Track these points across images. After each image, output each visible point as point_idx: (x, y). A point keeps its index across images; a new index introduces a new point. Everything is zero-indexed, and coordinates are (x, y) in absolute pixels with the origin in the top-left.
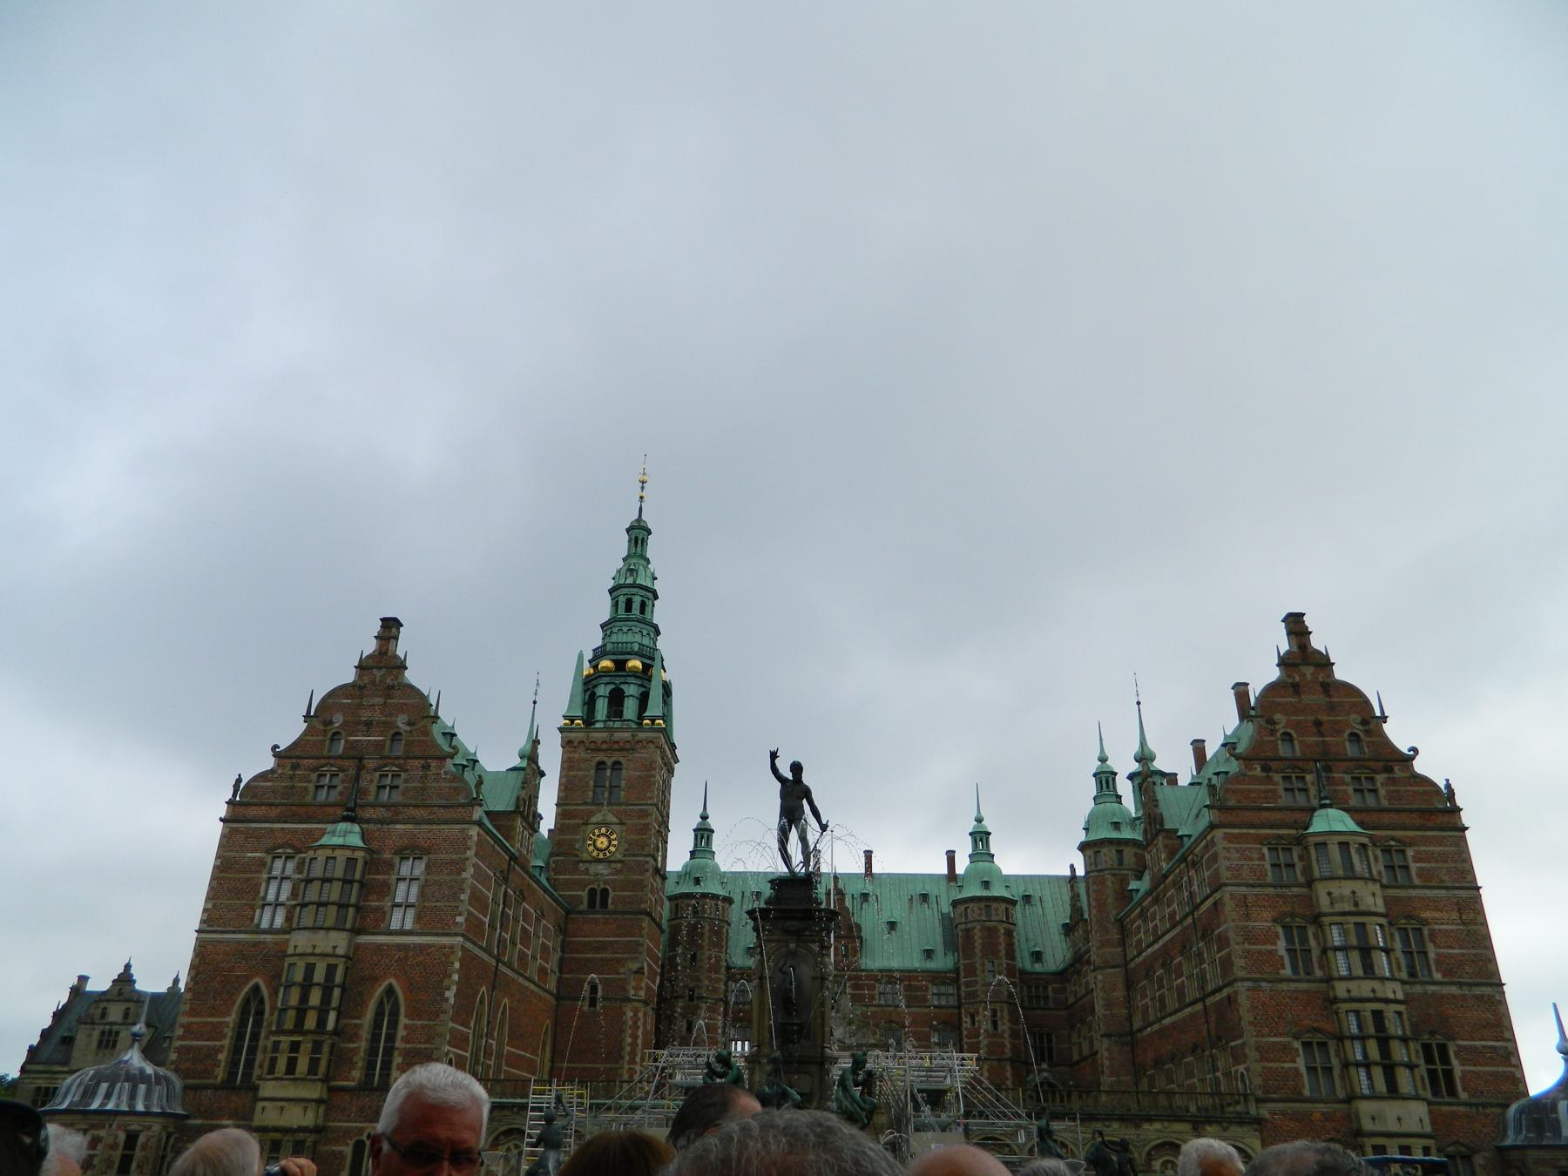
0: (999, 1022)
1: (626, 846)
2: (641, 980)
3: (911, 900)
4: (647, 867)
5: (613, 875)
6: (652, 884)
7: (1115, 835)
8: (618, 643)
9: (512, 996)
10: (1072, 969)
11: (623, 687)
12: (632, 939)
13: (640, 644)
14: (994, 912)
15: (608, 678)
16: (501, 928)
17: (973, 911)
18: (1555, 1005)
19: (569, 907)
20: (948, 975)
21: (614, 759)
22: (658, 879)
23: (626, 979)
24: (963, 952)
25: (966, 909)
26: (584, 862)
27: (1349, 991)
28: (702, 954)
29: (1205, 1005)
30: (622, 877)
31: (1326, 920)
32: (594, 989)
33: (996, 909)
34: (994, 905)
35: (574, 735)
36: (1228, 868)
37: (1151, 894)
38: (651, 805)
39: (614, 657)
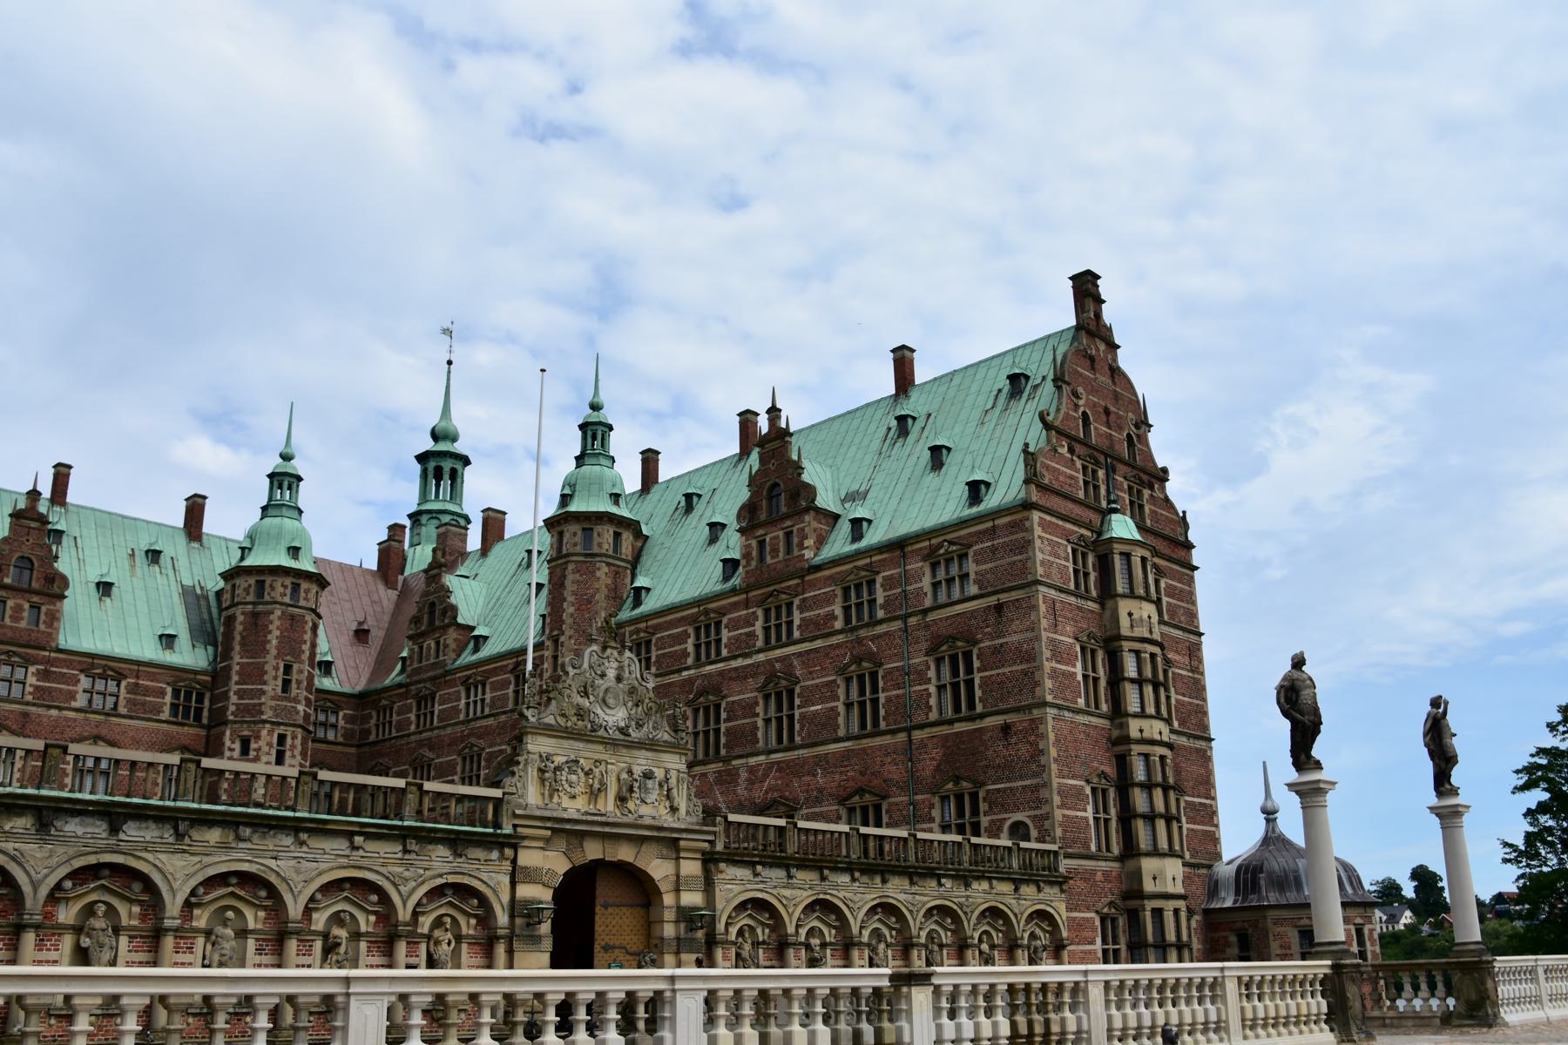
0: (288, 754)
3: (133, 555)
7: (614, 510)
10: (403, 690)
14: (303, 595)
17: (271, 586)
18: (1264, 763)
20: (199, 677)
24: (243, 644)
25: (260, 584)
27: (1141, 731)
29: (910, 740)
31: (1126, 645)
33: (307, 591)
34: (304, 585)
36: (1042, 562)
37: (747, 592)
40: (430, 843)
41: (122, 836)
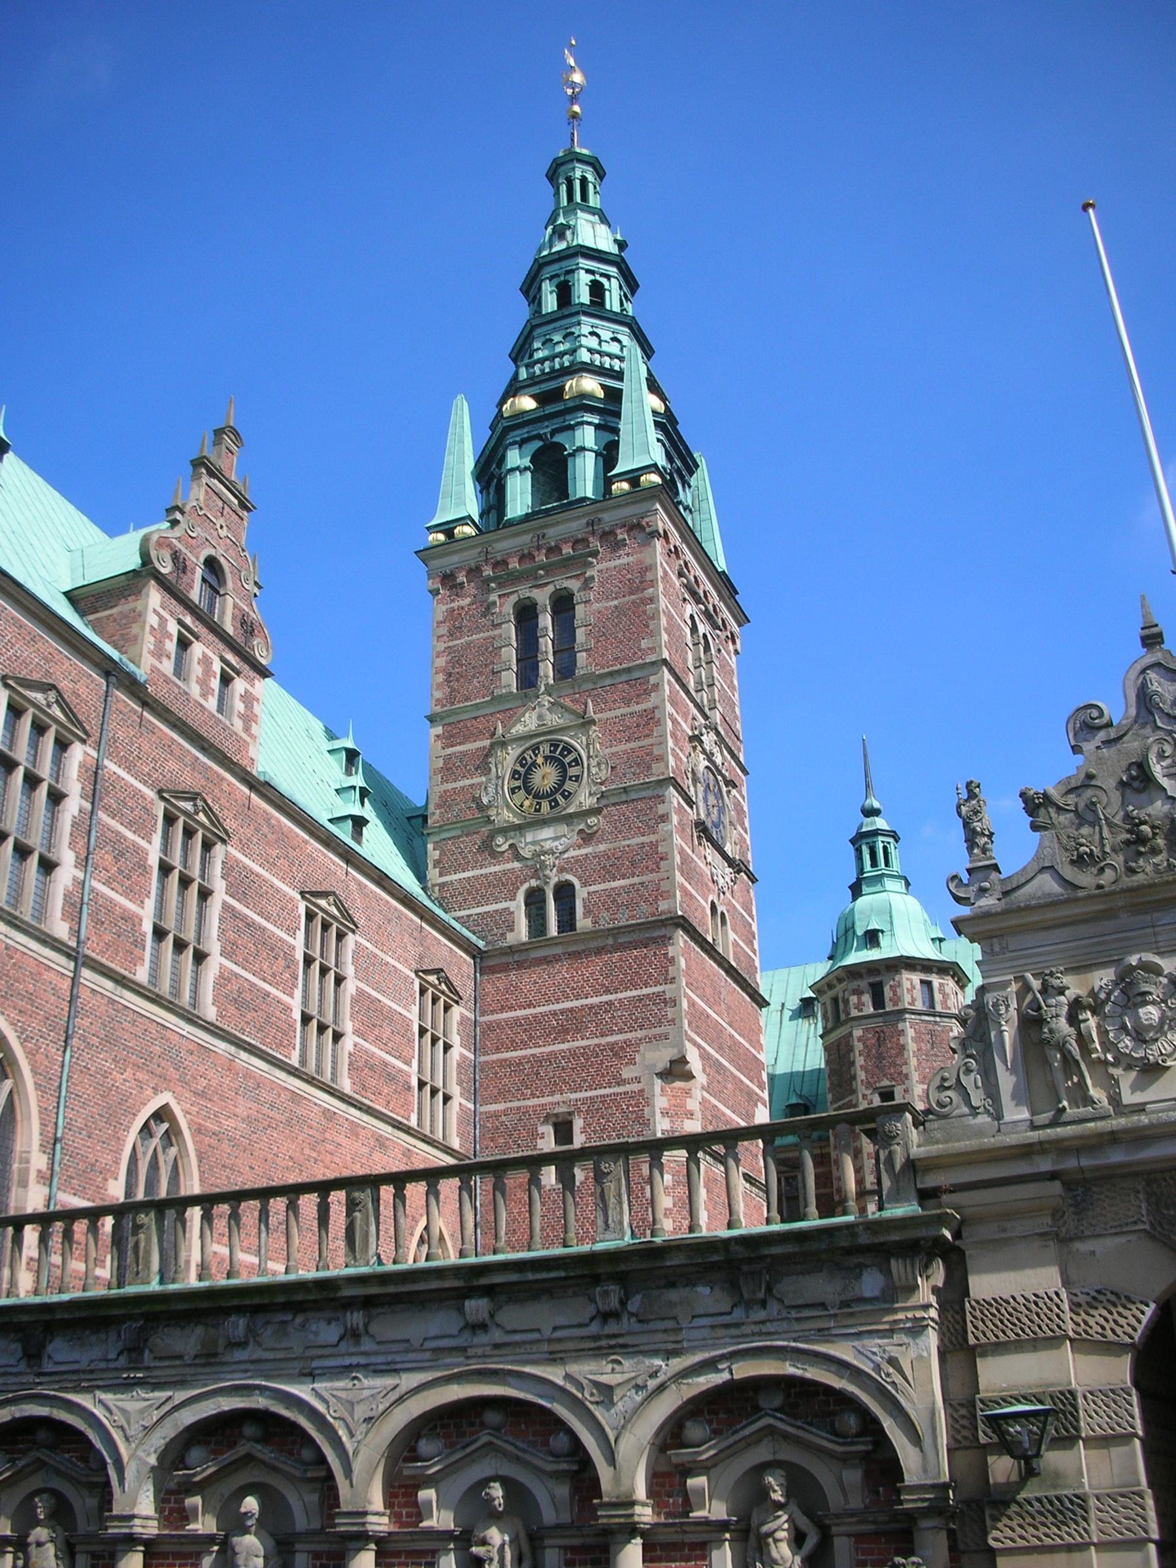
1: (604, 774)
2: (688, 1093)
4: (661, 809)
5: (579, 847)
6: (685, 859)
8: (542, 361)
9: (202, 1094)
11: (558, 438)
12: (645, 991)
13: (590, 350)
15: (525, 430)
16: (84, 862)
19: (481, 944)
21: (550, 589)
22: (710, 853)
23: (642, 1091)
26: (504, 831)
28: (906, 1091)
30: (602, 847)
32: (564, 1131)
35: (455, 558)
38: (653, 663)
39: (536, 390)
40: (672, 1285)
41: (48, 1367)
